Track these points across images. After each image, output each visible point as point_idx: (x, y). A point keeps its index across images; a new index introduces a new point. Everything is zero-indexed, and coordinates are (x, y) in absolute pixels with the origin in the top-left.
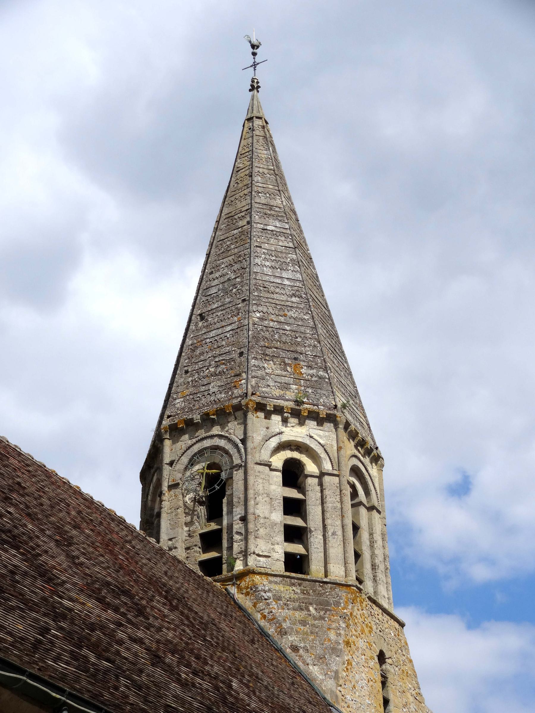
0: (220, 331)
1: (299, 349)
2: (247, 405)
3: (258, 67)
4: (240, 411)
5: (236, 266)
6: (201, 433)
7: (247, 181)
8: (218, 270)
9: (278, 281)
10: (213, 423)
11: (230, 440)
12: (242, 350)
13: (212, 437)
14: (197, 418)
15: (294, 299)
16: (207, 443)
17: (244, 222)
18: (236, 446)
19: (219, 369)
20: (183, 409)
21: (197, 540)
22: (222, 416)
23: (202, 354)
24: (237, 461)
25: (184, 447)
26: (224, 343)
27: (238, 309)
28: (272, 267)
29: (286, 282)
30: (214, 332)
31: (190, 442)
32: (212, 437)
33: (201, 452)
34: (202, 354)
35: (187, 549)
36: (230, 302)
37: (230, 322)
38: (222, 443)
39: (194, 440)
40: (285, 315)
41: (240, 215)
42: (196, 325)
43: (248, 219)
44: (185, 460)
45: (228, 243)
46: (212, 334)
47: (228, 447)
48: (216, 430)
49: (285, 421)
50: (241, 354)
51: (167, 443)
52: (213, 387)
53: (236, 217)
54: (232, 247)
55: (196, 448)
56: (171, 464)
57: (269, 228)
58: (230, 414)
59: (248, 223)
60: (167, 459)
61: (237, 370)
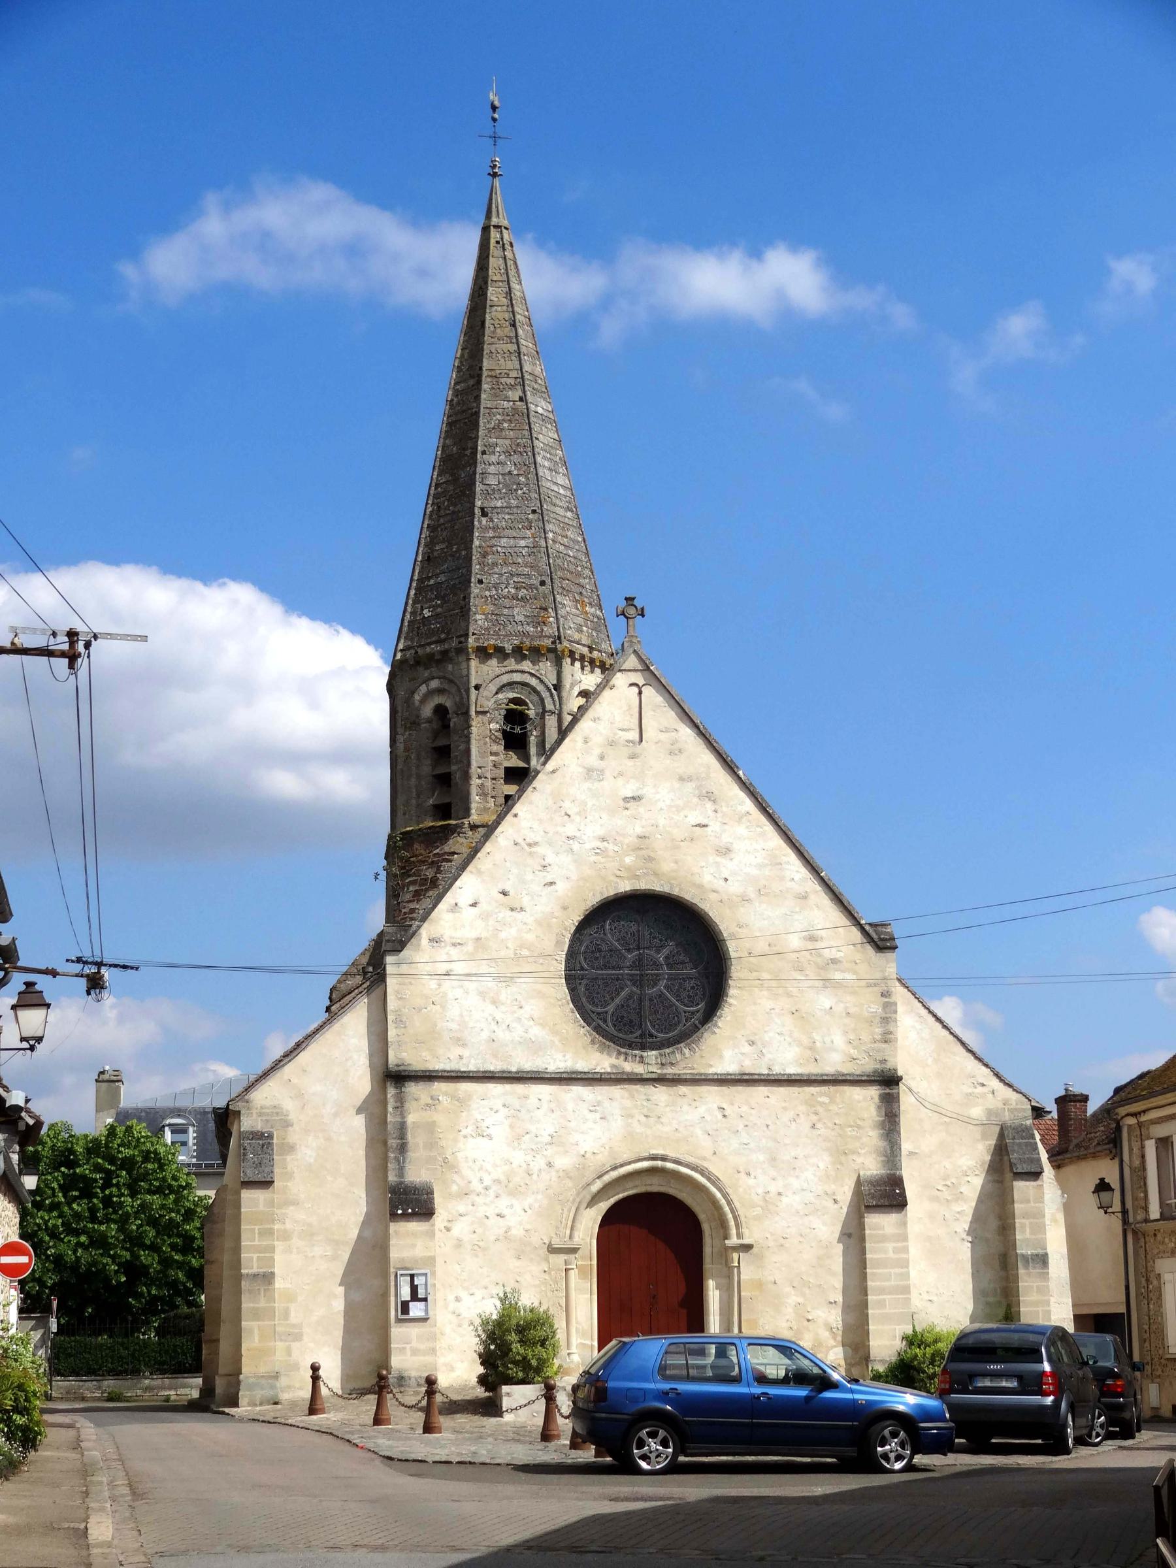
0: (512, 542)
1: (583, 581)
2: (563, 651)
3: (499, 141)
4: (557, 656)
5: (516, 458)
6: (511, 664)
7: (508, 331)
8: (494, 453)
9: (556, 488)
10: (524, 657)
11: (542, 681)
12: (543, 578)
13: (523, 672)
14: (508, 648)
15: (569, 514)
16: (517, 677)
17: (515, 394)
18: (550, 690)
19: (520, 594)
20: (487, 629)
21: (502, 773)
22: (536, 653)
23: (495, 564)
24: (549, 706)
25: (492, 676)
26: (520, 560)
27: (530, 521)
28: (550, 469)
29: (562, 491)
30: (505, 540)
31: (498, 671)
32: (523, 672)
33: (511, 685)
34: (495, 564)
35: (493, 779)
36: (517, 507)
37: (521, 534)
38: (533, 682)
39: (504, 670)
40: (566, 537)
41: (509, 381)
42: (480, 522)
43: (520, 393)
44: (493, 688)
45: (499, 417)
46: (504, 541)
47: (540, 688)
48: (526, 665)
49: (582, 668)
50: (543, 583)
51: (474, 663)
52: (519, 613)
53: (503, 380)
54: (506, 425)
55: (505, 679)
56: (477, 687)
57: (540, 410)
58: (543, 655)
59: (521, 399)
60: (473, 683)
61: (542, 603)
